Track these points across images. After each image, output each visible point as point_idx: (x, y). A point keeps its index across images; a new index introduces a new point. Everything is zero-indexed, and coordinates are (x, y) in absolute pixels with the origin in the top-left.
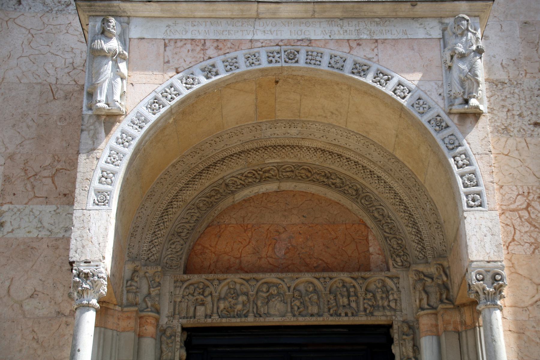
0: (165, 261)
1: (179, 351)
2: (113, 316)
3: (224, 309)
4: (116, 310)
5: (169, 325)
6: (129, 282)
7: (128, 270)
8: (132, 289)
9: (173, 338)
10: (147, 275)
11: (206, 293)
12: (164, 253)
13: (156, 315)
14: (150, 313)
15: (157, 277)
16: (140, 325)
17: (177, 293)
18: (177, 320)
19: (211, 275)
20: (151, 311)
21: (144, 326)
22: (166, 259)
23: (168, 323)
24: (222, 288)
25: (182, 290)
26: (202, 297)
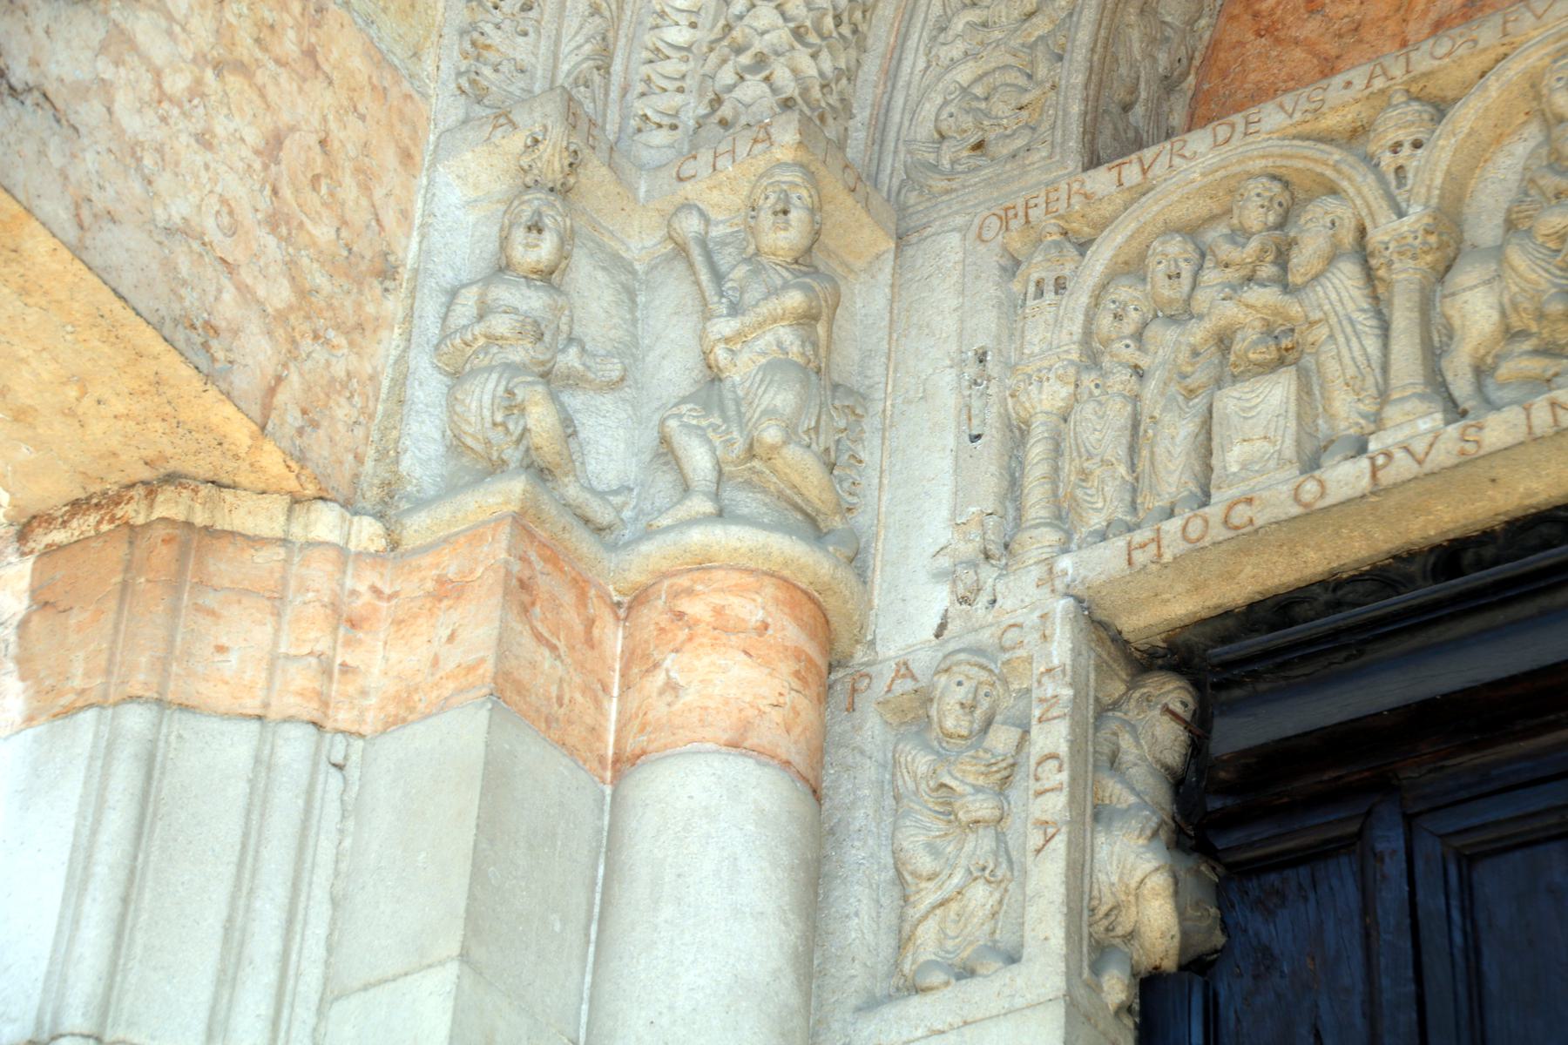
0: (925, 130)
1: (1060, 844)
2: (277, 600)
3: (1511, 334)
4: (311, 544)
5: (970, 639)
6: (469, 298)
7: (471, 204)
8: (492, 338)
9: (1002, 739)
10: (690, 225)
11: (1305, 258)
12: (913, 63)
13: (787, 548)
14: (697, 537)
15: (766, 219)
16: (624, 675)
17: (1036, 337)
18: (1036, 572)
19: (1338, 80)
20: (721, 514)
21: (656, 665)
22: (929, 109)
23: (952, 628)
24: (1477, 155)
25: (1081, 298)
26: (1264, 296)
